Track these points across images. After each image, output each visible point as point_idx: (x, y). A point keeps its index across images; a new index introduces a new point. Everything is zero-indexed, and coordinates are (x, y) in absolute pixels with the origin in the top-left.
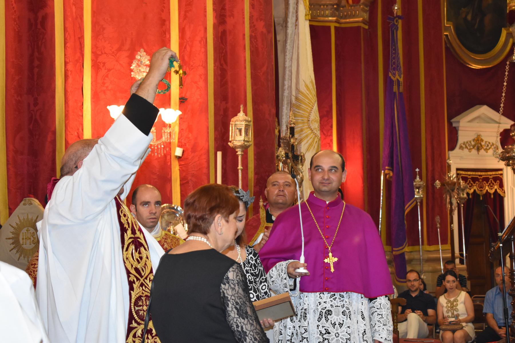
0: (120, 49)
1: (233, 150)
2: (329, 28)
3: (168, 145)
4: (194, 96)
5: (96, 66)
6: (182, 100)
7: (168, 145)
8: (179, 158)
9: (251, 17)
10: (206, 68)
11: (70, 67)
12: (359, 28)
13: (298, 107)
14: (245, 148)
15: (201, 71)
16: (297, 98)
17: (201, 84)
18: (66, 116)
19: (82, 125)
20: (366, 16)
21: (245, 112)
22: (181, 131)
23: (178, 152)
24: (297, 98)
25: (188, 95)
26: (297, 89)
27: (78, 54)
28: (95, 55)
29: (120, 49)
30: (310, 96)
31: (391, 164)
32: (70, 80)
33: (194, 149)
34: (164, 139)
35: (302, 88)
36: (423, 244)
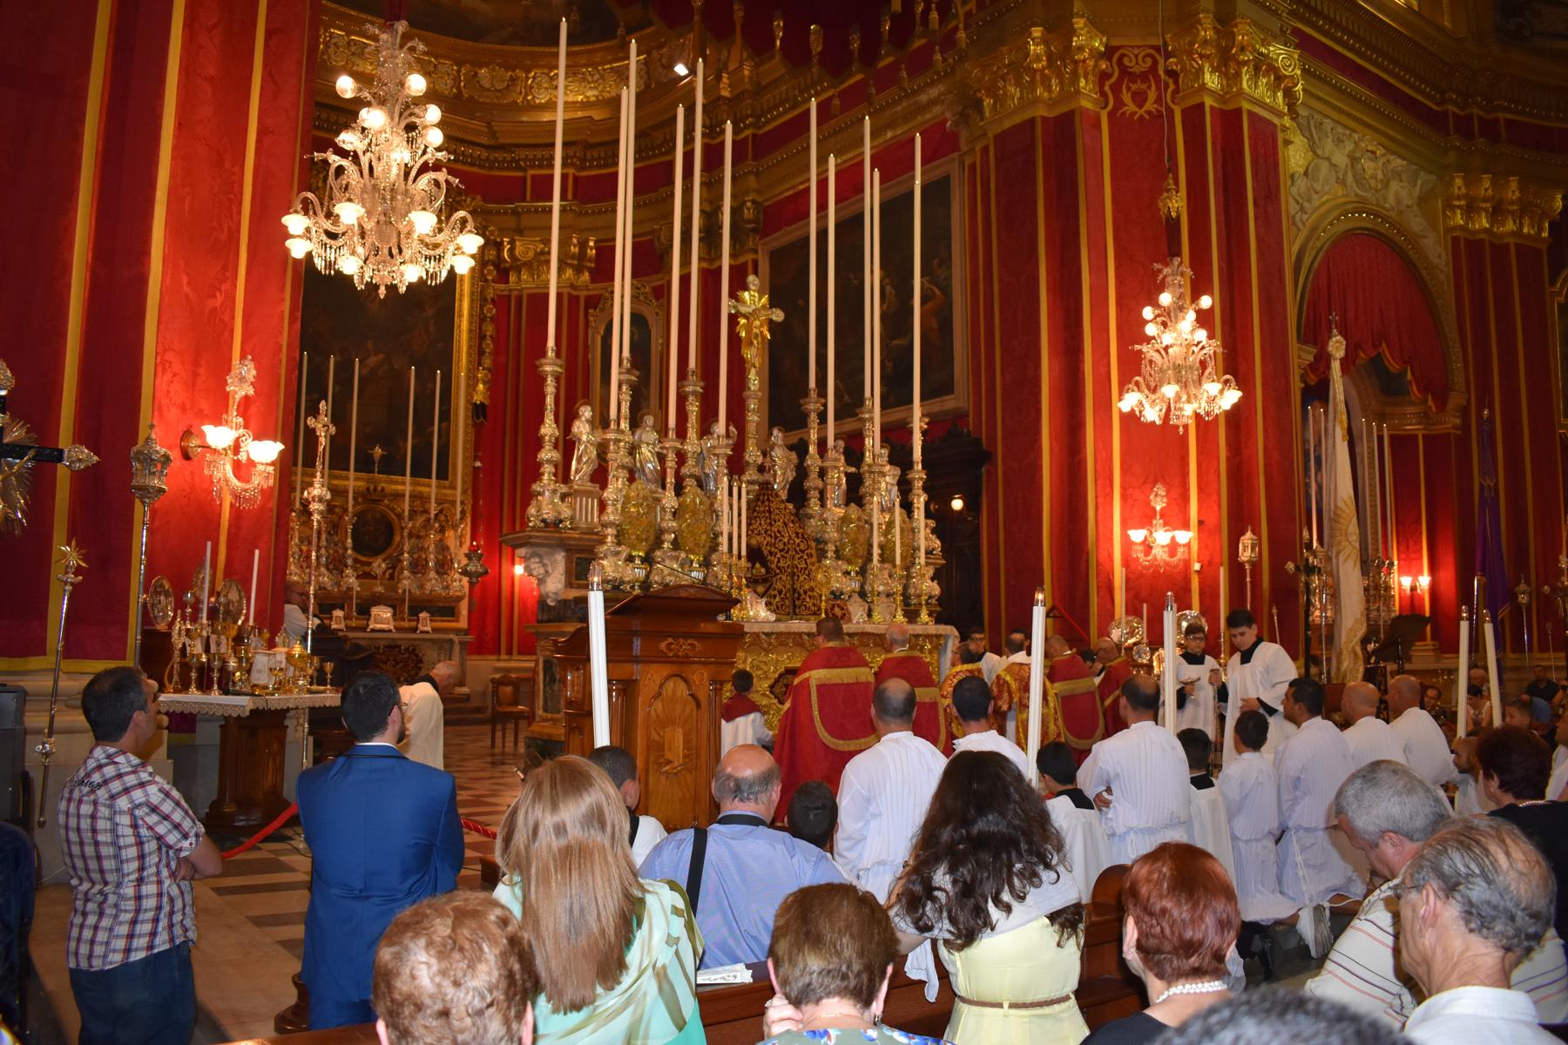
0: (1144, 483)
1: (1242, 565)
2: (1417, 436)
3: (1187, 564)
4: (1211, 521)
5: (1124, 498)
6: (1201, 523)
7: (1187, 564)
8: (1198, 572)
9: (1266, 448)
10: (1219, 495)
11: (1100, 500)
12: (1448, 434)
13: (1337, 522)
14: (1256, 565)
15: (1215, 497)
16: (1335, 513)
17: (1215, 508)
18: (1097, 540)
19: (1112, 545)
20: (1458, 421)
21: (1256, 532)
22: (1200, 548)
23: (1197, 567)
24: (1335, 513)
25: (1204, 518)
26: (1336, 505)
27: (1108, 490)
28: (1123, 488)
29: (1144, 483)
30: (1347, 511)
31: (1483, 570)
32: (1101, 511)
33: (1210, 563)
34: (1179, 556)
35: (1340, 504)
36: (1531, 650)
